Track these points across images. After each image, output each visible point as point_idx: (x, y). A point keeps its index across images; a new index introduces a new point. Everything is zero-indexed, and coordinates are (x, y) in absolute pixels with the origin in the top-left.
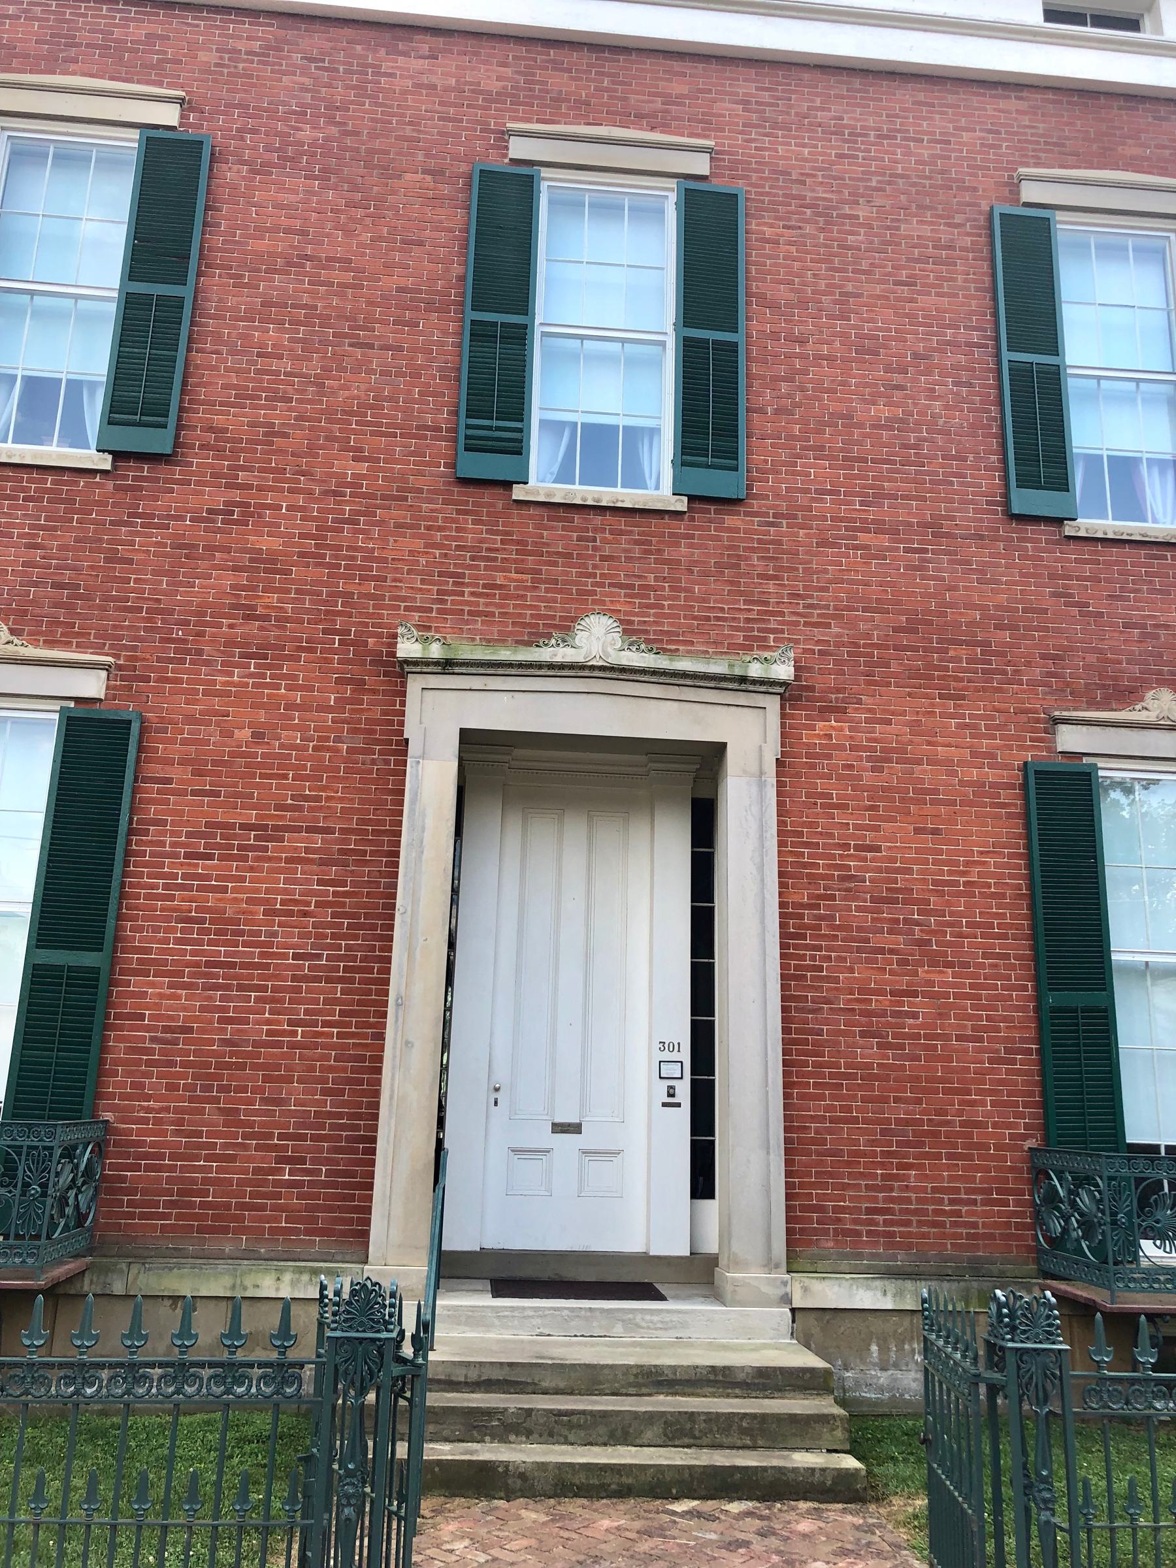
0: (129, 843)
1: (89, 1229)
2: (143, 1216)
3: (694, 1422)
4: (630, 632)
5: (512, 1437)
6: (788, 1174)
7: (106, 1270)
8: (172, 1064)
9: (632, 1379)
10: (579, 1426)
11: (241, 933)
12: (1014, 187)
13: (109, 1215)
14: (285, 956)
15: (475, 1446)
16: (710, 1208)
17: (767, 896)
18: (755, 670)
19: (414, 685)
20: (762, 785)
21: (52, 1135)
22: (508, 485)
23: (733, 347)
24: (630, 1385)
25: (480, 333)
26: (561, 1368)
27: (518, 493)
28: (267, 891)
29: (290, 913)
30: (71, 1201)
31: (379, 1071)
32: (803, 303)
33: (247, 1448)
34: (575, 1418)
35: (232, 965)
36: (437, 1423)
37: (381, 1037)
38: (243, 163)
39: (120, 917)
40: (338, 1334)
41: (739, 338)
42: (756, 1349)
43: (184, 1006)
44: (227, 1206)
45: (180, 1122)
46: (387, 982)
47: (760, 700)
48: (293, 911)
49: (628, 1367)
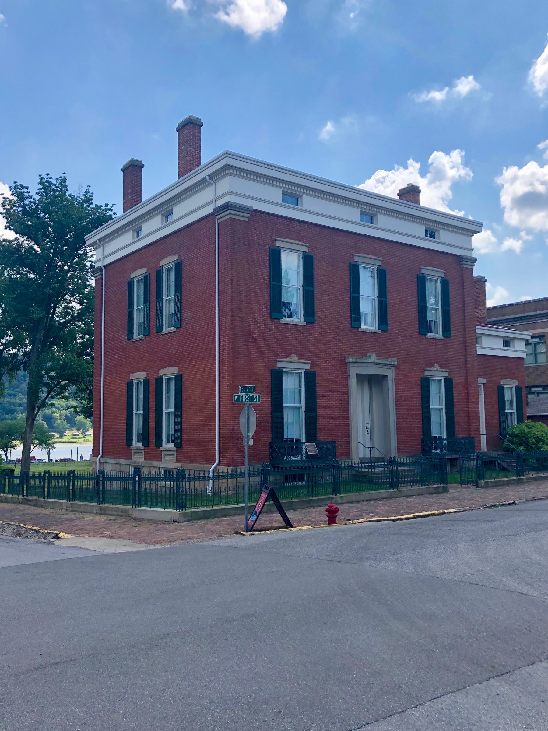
4: (378, 356)
12: (420, 269)
18: (393, 363)
22: (358, 328)
23: (386, 302)
47: (392, 368)
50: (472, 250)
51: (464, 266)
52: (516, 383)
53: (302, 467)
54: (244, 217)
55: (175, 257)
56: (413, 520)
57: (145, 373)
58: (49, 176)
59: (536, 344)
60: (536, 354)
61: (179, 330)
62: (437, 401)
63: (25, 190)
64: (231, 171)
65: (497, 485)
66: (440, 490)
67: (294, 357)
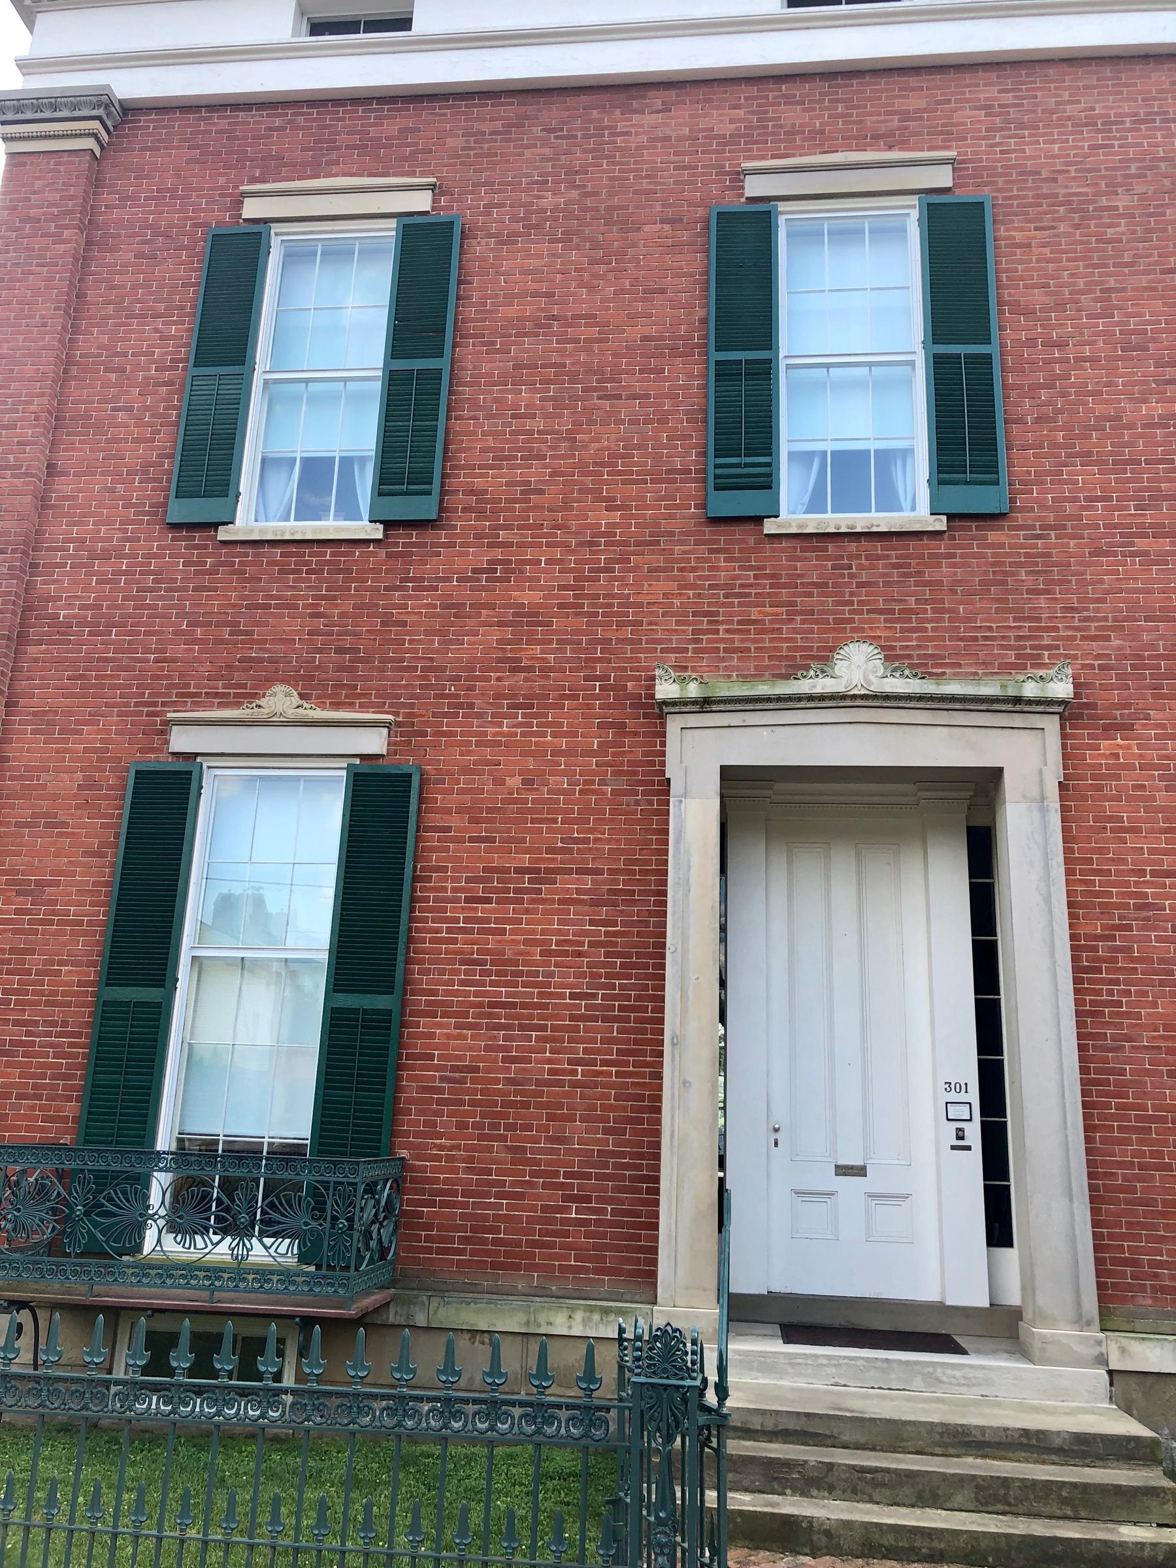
0: (414, 890)
1: (392, 1262)
2: (440, 1251)
3: (1008, 1488)
4: (892, 657)
5: (814, 1492)
6: (1095, 1224)
7: (409, 1303)
8: (461, 1103)
9: (937, 1438)
10: (883, 1485)
11: (520, 974)
13: (410, 1249)
14: (562, 996)
15: (775, 1498)
16: (1009, 1257)
17: (1056, 927)
18: (1030, 690)
19: (673, 725)
20: (1044, 811)
21: (356, 1172)
22: (758, 520)
24: (937, 1444)
25: (725, 372)
26: (860, 1422)
27: (770, 527)
28: (543, 932)
29: (565, 954)
30: (374, 1235)
31: (658, 1110)
32: (1060, 306)
33: (550, 1484)
34: (879, 1476)
35: (513, 1005)
36: (735, 1471)
37: (659, 1076)
38: (490, 236)
39: (408, 961)
40: (642, 1379)
41: (993, 349)
42: (1072, 1412)
43: (469, 1046)
44: (518, 1243)
45: (470, 1160)
46: (661, 1021)
48: (569, 951)
49: (932, 1424)
67: (281, 700)
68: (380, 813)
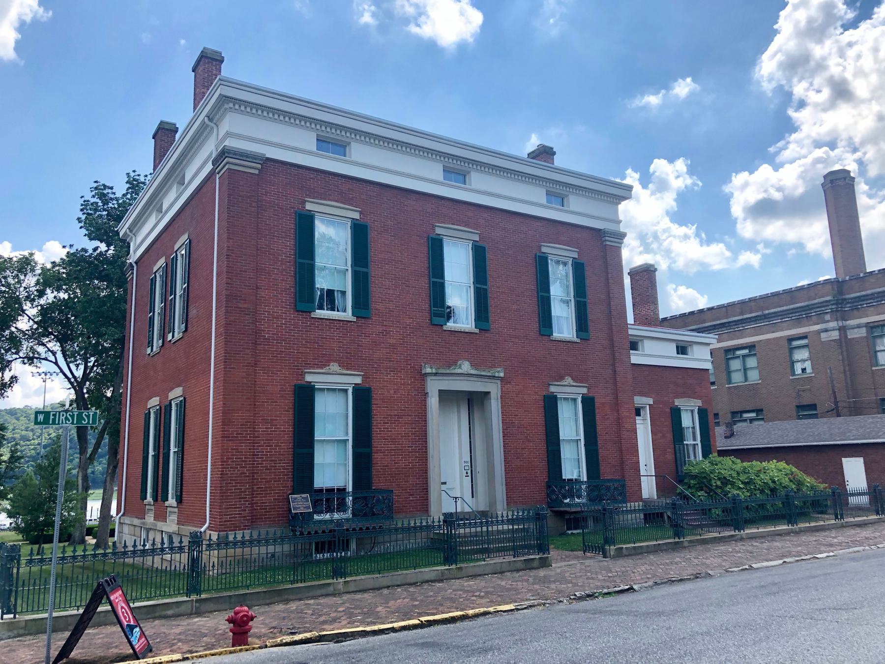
12: (540, 247)
18: (497, 375)
27: (445, 328)
32: (499, 277)
50: (620, 222)
51: (608, 243)
52: (699, 403)
53: (354, 529)
54: (253, 169)
55: (185, 237)
56: (420, 630)
57: (158, 398)
58: (137, 173)
59: (744, 356)
60: (745, 370)
61: (186, 334)
62: (571, 426)
63: (110, 191)
64: (231, 105)
65: (637, 552)
66: (536, 564)
67: (335, 367)
68: (362, 400)
